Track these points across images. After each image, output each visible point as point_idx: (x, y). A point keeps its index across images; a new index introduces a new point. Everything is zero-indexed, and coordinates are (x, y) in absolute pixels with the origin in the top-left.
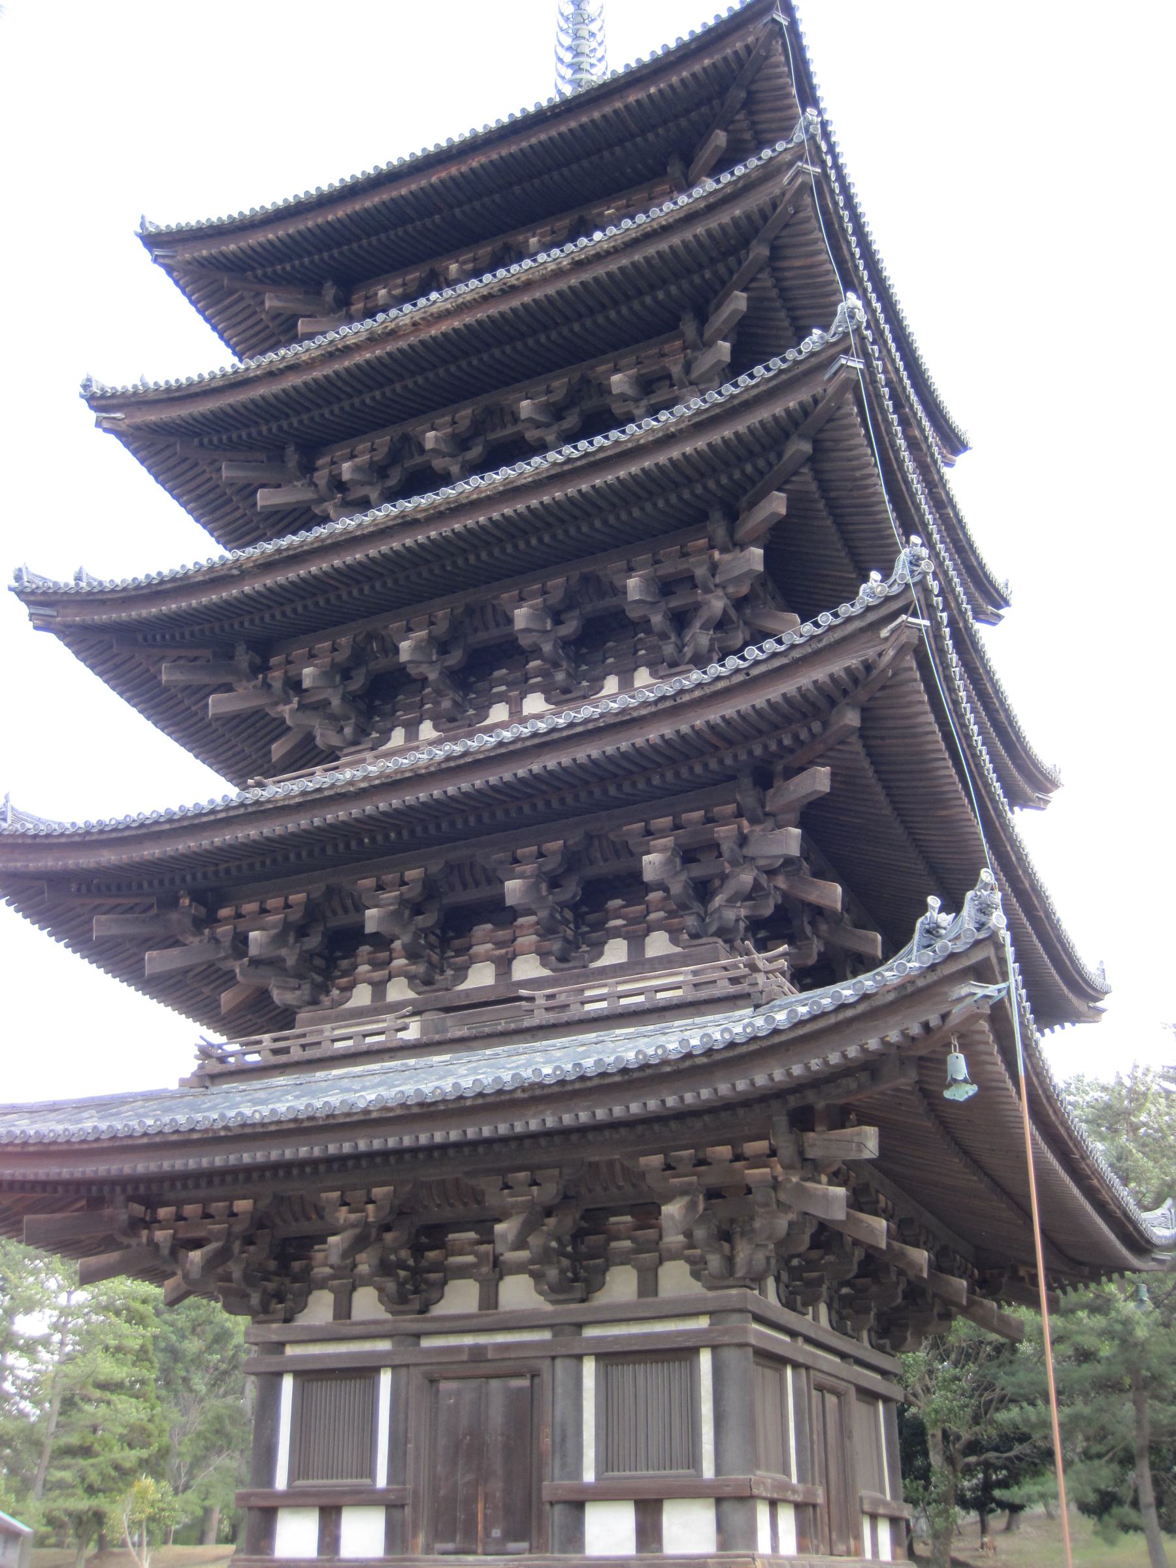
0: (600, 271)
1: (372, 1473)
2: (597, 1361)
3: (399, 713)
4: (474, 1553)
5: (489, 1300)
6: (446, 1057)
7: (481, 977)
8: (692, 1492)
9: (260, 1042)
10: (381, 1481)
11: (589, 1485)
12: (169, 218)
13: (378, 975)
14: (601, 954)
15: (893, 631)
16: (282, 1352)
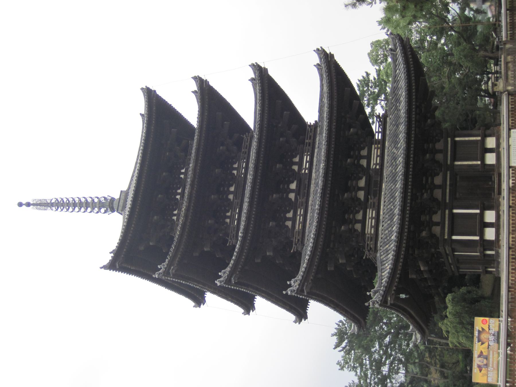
0: (204, 129)
1: (476, 214)
2: (455, 161)
3: (281, 223)
4: (494, 187)
5: (439, 187)
6: (384, 184)
7: (361, 195)
8: (483, 142)
9: (368, 237)
10: (478, 211)
11: (481, 163)
12: (108, 258)
13: (353, 222)
14: (363, 166)
15: (330, 58)
16: (446, 239)
